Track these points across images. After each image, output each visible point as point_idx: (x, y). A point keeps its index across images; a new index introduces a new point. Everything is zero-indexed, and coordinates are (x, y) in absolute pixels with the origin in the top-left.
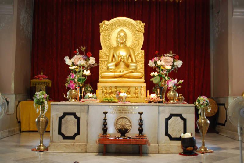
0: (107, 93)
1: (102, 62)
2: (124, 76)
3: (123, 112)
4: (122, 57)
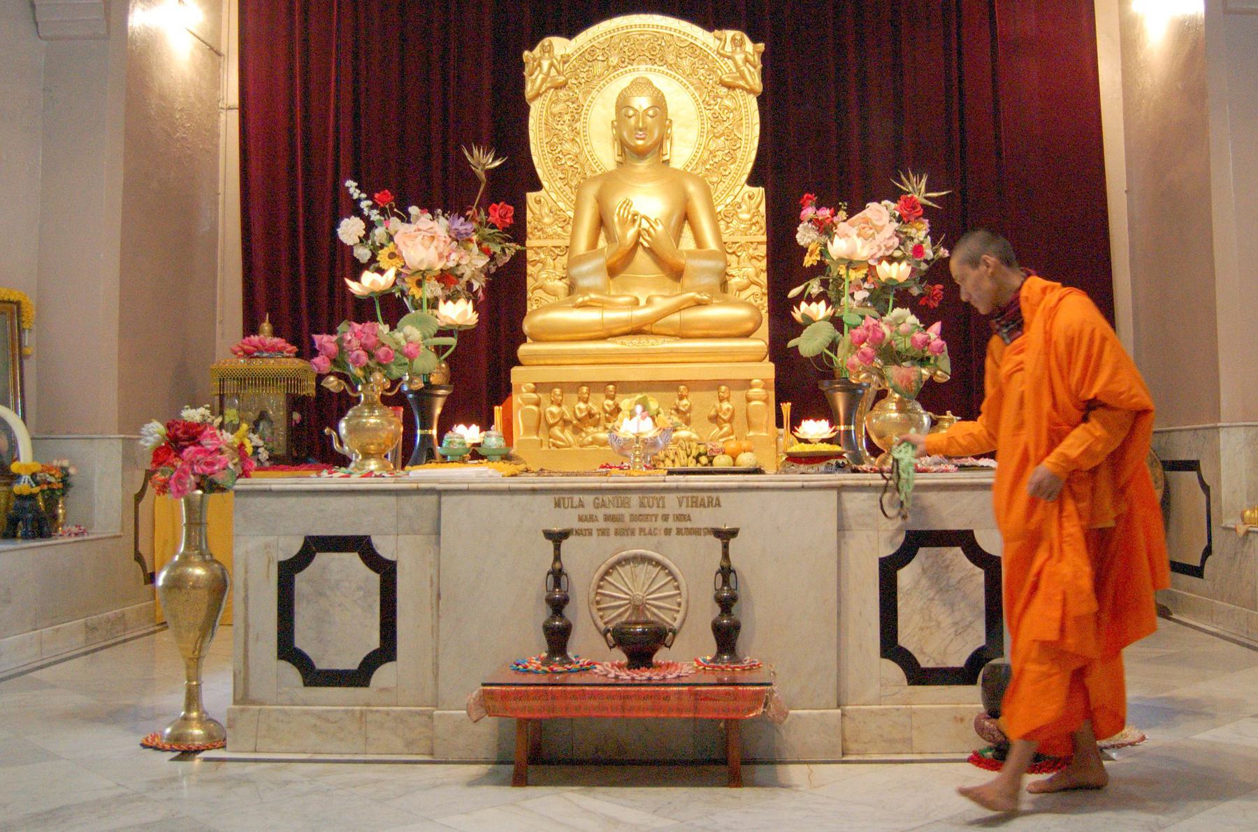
0: (566, 423)
1: (542, 256)
2: (655, 330)
3: (637, 525)
4: (645, 225)
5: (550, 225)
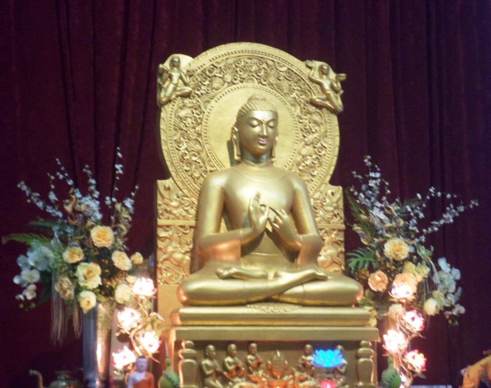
2: (285, 299)
5: (176, 208)
